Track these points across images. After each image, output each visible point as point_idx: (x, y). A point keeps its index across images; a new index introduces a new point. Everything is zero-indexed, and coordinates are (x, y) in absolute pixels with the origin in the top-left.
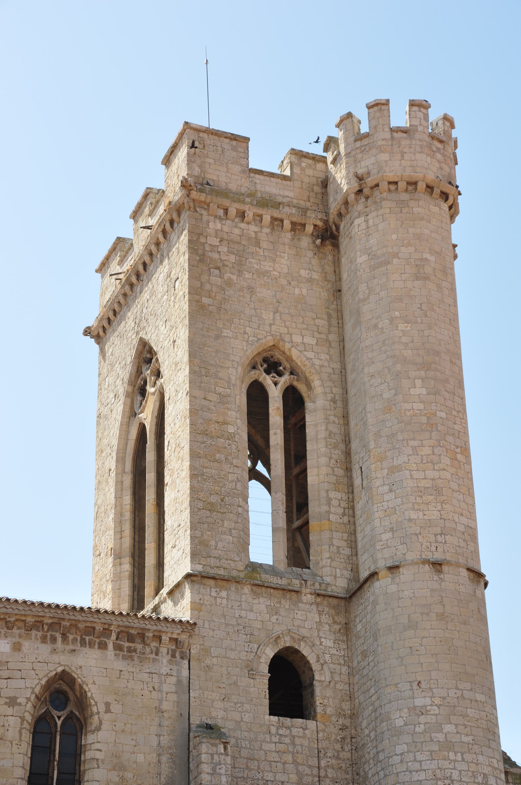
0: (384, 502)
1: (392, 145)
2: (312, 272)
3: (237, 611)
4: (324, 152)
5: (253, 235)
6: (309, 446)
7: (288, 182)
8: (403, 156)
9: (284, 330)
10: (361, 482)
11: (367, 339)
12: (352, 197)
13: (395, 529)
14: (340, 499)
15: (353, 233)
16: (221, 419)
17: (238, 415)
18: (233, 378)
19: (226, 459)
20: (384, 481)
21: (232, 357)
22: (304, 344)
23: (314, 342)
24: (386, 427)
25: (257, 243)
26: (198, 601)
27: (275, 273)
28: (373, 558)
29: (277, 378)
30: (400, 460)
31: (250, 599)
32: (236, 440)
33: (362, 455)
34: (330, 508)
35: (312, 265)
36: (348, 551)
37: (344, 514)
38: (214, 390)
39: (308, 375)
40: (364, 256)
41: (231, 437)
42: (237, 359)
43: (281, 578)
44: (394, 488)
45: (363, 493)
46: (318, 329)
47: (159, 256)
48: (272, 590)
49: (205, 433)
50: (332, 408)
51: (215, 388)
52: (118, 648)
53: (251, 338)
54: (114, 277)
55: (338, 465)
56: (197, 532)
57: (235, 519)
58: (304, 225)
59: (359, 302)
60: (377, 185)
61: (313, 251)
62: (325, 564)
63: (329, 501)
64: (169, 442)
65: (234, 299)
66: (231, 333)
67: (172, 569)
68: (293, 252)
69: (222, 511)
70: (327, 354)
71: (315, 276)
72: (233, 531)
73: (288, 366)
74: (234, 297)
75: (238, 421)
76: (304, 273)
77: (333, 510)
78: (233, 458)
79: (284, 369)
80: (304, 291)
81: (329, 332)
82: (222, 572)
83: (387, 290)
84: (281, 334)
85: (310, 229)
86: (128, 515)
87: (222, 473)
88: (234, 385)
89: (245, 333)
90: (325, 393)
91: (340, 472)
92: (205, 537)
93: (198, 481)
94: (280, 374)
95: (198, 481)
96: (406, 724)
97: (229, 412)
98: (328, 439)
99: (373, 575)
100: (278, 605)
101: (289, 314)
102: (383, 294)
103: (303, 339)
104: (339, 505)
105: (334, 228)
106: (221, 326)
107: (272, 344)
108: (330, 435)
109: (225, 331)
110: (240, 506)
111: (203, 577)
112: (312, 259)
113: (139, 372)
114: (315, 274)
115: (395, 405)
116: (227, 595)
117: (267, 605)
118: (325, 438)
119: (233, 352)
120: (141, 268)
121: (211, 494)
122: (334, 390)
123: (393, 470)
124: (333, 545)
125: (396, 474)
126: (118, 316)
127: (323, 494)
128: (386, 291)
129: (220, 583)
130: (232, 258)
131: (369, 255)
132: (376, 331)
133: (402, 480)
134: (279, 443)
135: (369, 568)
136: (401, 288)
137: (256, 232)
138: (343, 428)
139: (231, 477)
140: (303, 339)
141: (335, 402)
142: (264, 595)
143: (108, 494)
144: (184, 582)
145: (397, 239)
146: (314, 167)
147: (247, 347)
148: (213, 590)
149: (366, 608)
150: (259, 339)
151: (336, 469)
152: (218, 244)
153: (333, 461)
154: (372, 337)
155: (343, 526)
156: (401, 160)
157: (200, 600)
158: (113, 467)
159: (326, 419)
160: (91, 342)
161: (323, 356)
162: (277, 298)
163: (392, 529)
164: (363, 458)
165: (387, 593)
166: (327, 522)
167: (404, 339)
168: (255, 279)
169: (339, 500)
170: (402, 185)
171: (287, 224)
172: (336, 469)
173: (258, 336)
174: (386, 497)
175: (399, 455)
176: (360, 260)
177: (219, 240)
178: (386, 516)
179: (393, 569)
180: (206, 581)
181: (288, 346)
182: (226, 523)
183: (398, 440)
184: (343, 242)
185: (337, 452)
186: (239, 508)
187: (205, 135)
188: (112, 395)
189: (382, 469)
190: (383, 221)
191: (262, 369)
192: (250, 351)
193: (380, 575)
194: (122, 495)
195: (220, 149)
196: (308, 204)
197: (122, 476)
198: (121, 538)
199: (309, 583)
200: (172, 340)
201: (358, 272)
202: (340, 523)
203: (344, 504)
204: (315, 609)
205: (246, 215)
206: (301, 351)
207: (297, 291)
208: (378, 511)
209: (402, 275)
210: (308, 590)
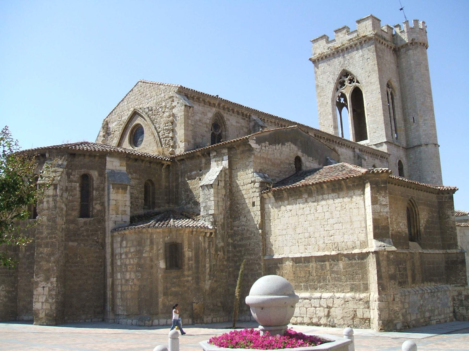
33: (414, 114)
52: (380, 159)
85: (392, 48)
99: (420, 145)
113: (341, 78)
123: (425, 120)
163: (425, 135)
174: (423, 127)
179: (427, 145)
193: (423, 145)
200: (367, 75)
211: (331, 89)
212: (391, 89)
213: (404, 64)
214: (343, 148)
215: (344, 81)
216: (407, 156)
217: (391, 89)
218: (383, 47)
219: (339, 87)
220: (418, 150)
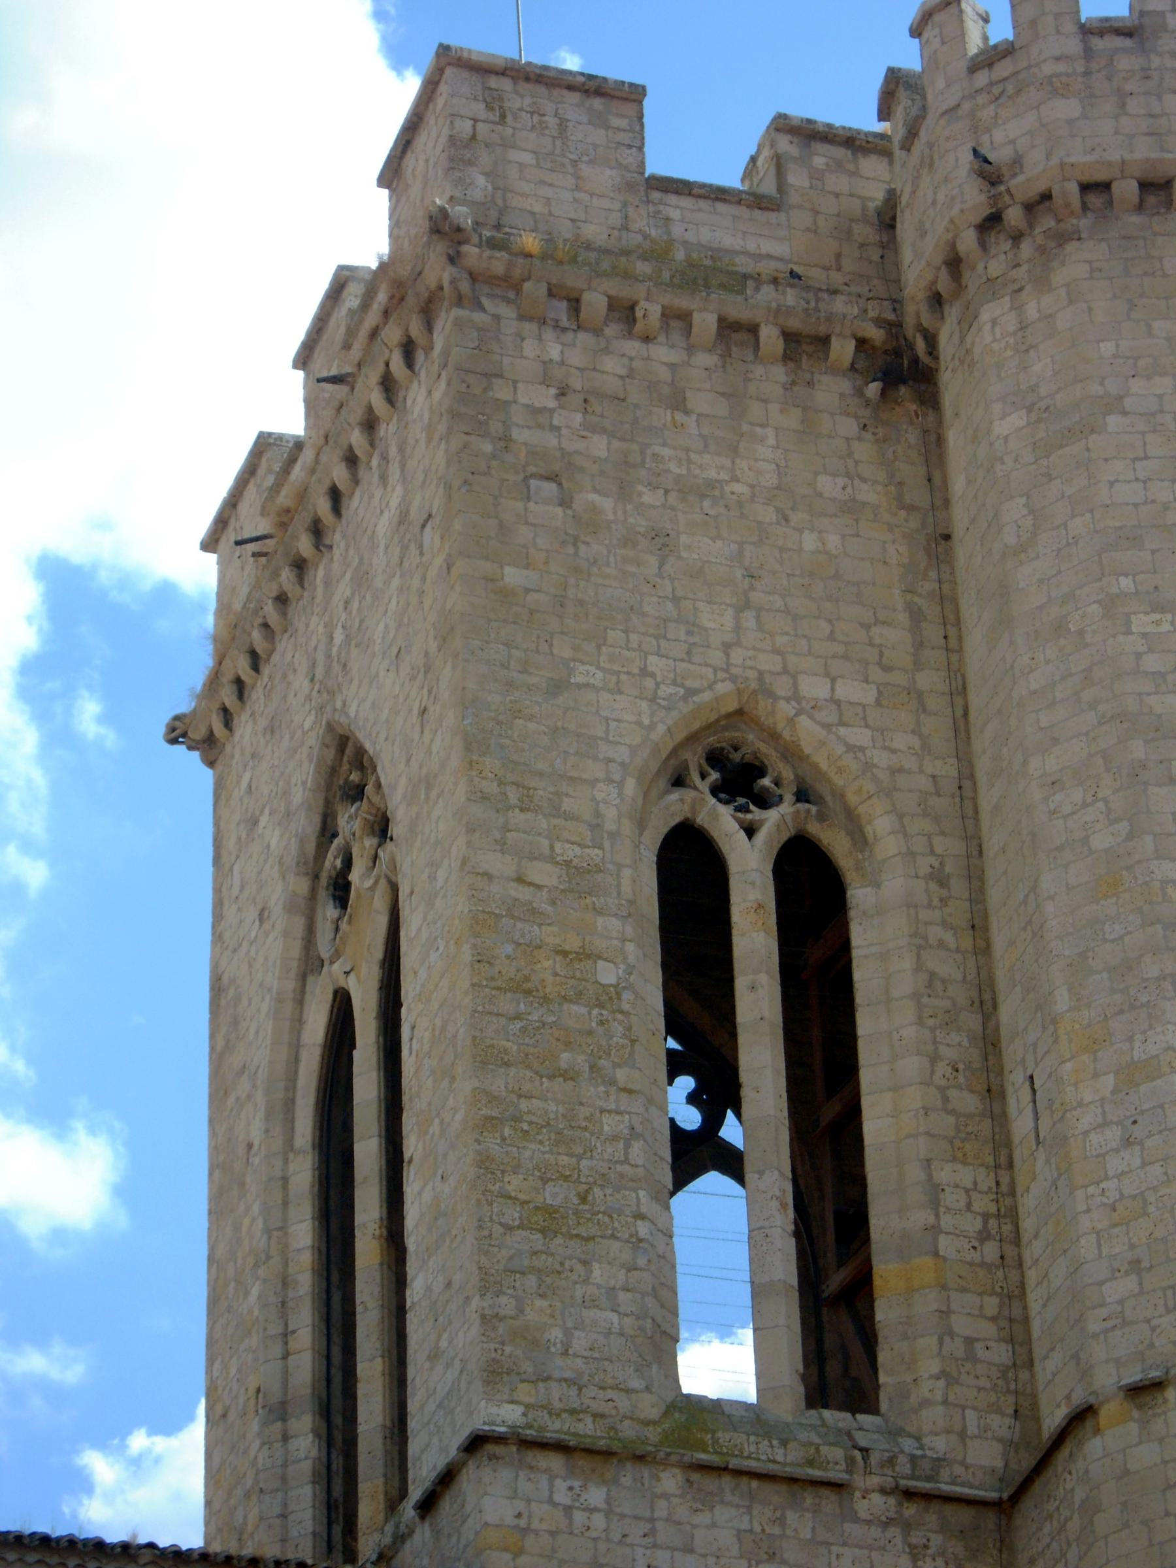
0: (1107, 1178)
1: (1087, 73)
2: (857, 482)
3: (639, 1551)
4: (881, 119)
5: (665, 374)
6: (865, 1024)
7: (772, 216)
8: (1123, 106)
9: (769, 663)
10: (1031, 1124)
11: (1032, 671)
12: (968, 241)
13: (1145, 1264)
14: (970, 1185)
15: (977, 351)
16: (572, 943)
17: (629, 930)
18: (610, 813)
19: (591, 1068)
20: (1104, 1113)
21: (604, 750)
22: (838, 703)
23: (867, 695)
24: (1105, 941)
25: (678, 403)
26: (510, 1520)
27: (739, 488)
28: (1078, 1364)
29: (756, 814)
31: (683, 1512)
32: (626, 1006)
34: (937, 1216)
35: (857, 462)
36: (1001, 1354)
37: (984, 1236)
38: (547, 852)
39: (852, 799)
40: (1014, 416)
41: (607, 998)
42: (623, 754)
43: (784, 1443)
44: (1138, 1132)
45: (1041, 1156)
46: (881, 654)
47: (375, 462)
48: (755, 1484)
49: (522, 987)
50: (936, 902)
51: (552, 848)
53: (665, 690)
54: (252, 547)
55: (961, 1079)
56: (503, 1300)
57: (626, 1256)
58: (824, 341)
60: (1046, 197)
61: (856, 417)
62: (928, 1395)
63: (934, 1194)
64: (413, 1028)
65: (607, 570)
66: (600, 675)
67: (432, 1426)
68: (792, 420)
69: (582, 1231)
70: (913, 732)
71: (868, 494)
72: (622, 1296)
73: (787, 774)
74: (608, 565)
75: (630, 947)
76: (828, 485)
77: (946, 1221)
78: (616, 1065)
79: (777, 783)
80: (833, 541)
81: (918, 666)
82: (587, 1428)
83: (1092, 511)
84: (761, 673)
85: (843, 350)
86: (305, 1281)
87: (584, 1111)
88: (613, 836)
89: (645, 672)
90: (911, 854)
91: (969, 1102)
92: (531, 1315)
93: (504, 1139)
94: (764, 802)
95: (504, 1139)
97: (600, 921)
98: (925, 1000)
100: (776, 1530)
101: (787, 611)
102: (1078, 525)
103: (833, 689)
104: (969, 1206)
105: (920, 345)
106: (567, 654)
107: (731, 706)
108: (930, 985)
109: (581, 668)
110: (642, 1217)
111: (527, 1444)
112: (855, 445)
113: (327, 832)
114: (865, 487)
115: (1127, 868)
116: (608, 1501)
117: (739, 1531)
118: (916, 996)
119: (607, 731)
120: (323, 506)
121: (545, 1181)
122: (940, 844)
124: (952, 1335)
125: (1142, 1088)
126: (266, 670)
127: (915, 1173)
128: (1088, 515)
129: (582, 1462)
130: (599, 446)
131: (1030, 409)
132: (1062, 642)
133: (1162, 1106)
134: (766, 1014)
135: (1068, 1397)
136: (1136, 505)
137: (672, 366)
138: (971, 962)
139: (609, 1124)
140: (833, 689)
141: (943, 882)
142: (728, 1497)
143: (246, 1222)
144: (464, 1463)
145: (1115, 356)
146: (851, 167)
147: (652, 715)
148: (561, 1485)
149: (1063, 1528)
150: (691, 692)
151: (953, 1093)
152: (552, 404)
153: (942, 1068)
154: (1048, 662)
155: (982, 1272)
156: (1116, 117)
157: (519, 1515)
158: (257, 1136)
159: (915, 935)
160: (188, 759)
161: (901, 741)
162: (747, 562)
163: (1135, 1266)
164: (1035, 1045)
165: (1127, 1472)
166: (929, 1261)
167: (1152, 663)
168: (673, 509)
169: (967, 1191)
170: (1126, 190)
171: (769, 336)
172: (953, 1093)
173: (688, 683)
174: (1114, 1165)
175: (1151, 1027)
176: (1002, 428)
177: (553, 391)
178: (1115, 1225)
180: (532, 1456)
181: (786, 709)
182: (598, 1273)
183: (1145, 980)
184: (951, 383)
185: (954, 1038)
186: (639, 1223)
187: (506, 84)
188: (252, 914)
189: (1096, 1075)
190: (1071, 302)
191: (704, 786)
192: (661, 729)
193: (1106, 1413)
194: (285, 1220)
195: (551, 120)
196: (837, 279)
197: (286, 1161)
198: (285, 1356)
199: (874, 1459)
200: (416, 711)
201: (998, 467)
202: (971, 1264)
203: (982, 1203)
204: (898, 1540)
205: (639, 313)
206: (827, 726)
207: (809, 541)
208: (1088, 1211)
209: (1138, 464)
210: (874, 1481)
218: (663, 353)
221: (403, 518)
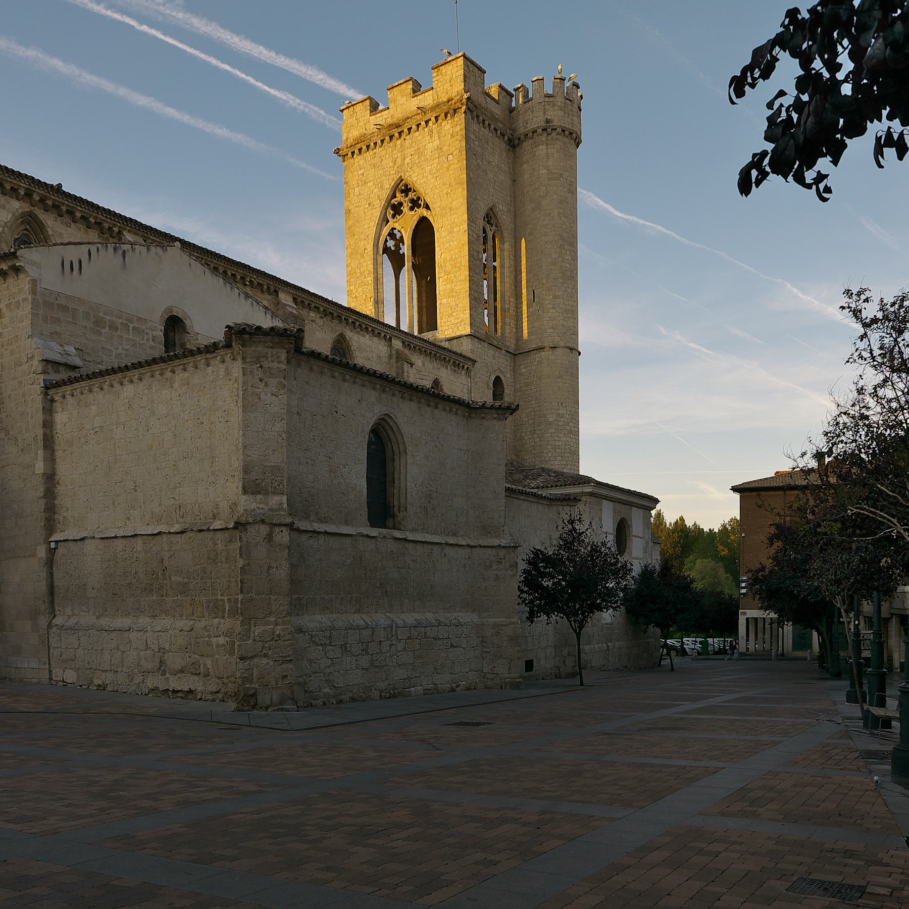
30: (560, 293)
33: (535, 284)
59: (540, 197)
91: (513, 287)
96: (554, 421)
99: (541, 349)
123: (555, 297)
161: (509, 220)
171: (499, 132)
200: (445, 192)
211: (374, 218)
212: (494, 228)
213: (527, 176)
214: (364, 336)
215: (401, 204)
216: (514, 369)
217: (494, 228)
218: (486, 131)
219: (390, 217)
220: (535, 357)
221: (439, 148)
